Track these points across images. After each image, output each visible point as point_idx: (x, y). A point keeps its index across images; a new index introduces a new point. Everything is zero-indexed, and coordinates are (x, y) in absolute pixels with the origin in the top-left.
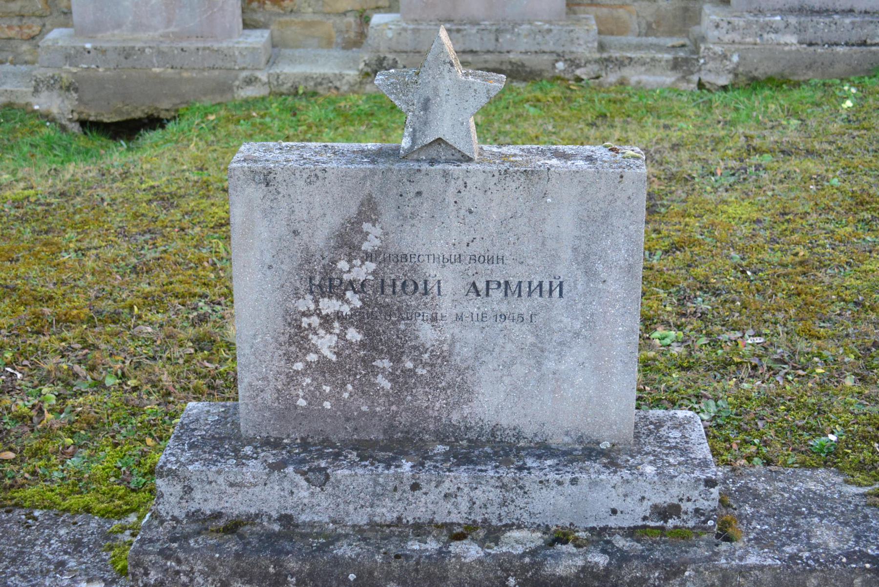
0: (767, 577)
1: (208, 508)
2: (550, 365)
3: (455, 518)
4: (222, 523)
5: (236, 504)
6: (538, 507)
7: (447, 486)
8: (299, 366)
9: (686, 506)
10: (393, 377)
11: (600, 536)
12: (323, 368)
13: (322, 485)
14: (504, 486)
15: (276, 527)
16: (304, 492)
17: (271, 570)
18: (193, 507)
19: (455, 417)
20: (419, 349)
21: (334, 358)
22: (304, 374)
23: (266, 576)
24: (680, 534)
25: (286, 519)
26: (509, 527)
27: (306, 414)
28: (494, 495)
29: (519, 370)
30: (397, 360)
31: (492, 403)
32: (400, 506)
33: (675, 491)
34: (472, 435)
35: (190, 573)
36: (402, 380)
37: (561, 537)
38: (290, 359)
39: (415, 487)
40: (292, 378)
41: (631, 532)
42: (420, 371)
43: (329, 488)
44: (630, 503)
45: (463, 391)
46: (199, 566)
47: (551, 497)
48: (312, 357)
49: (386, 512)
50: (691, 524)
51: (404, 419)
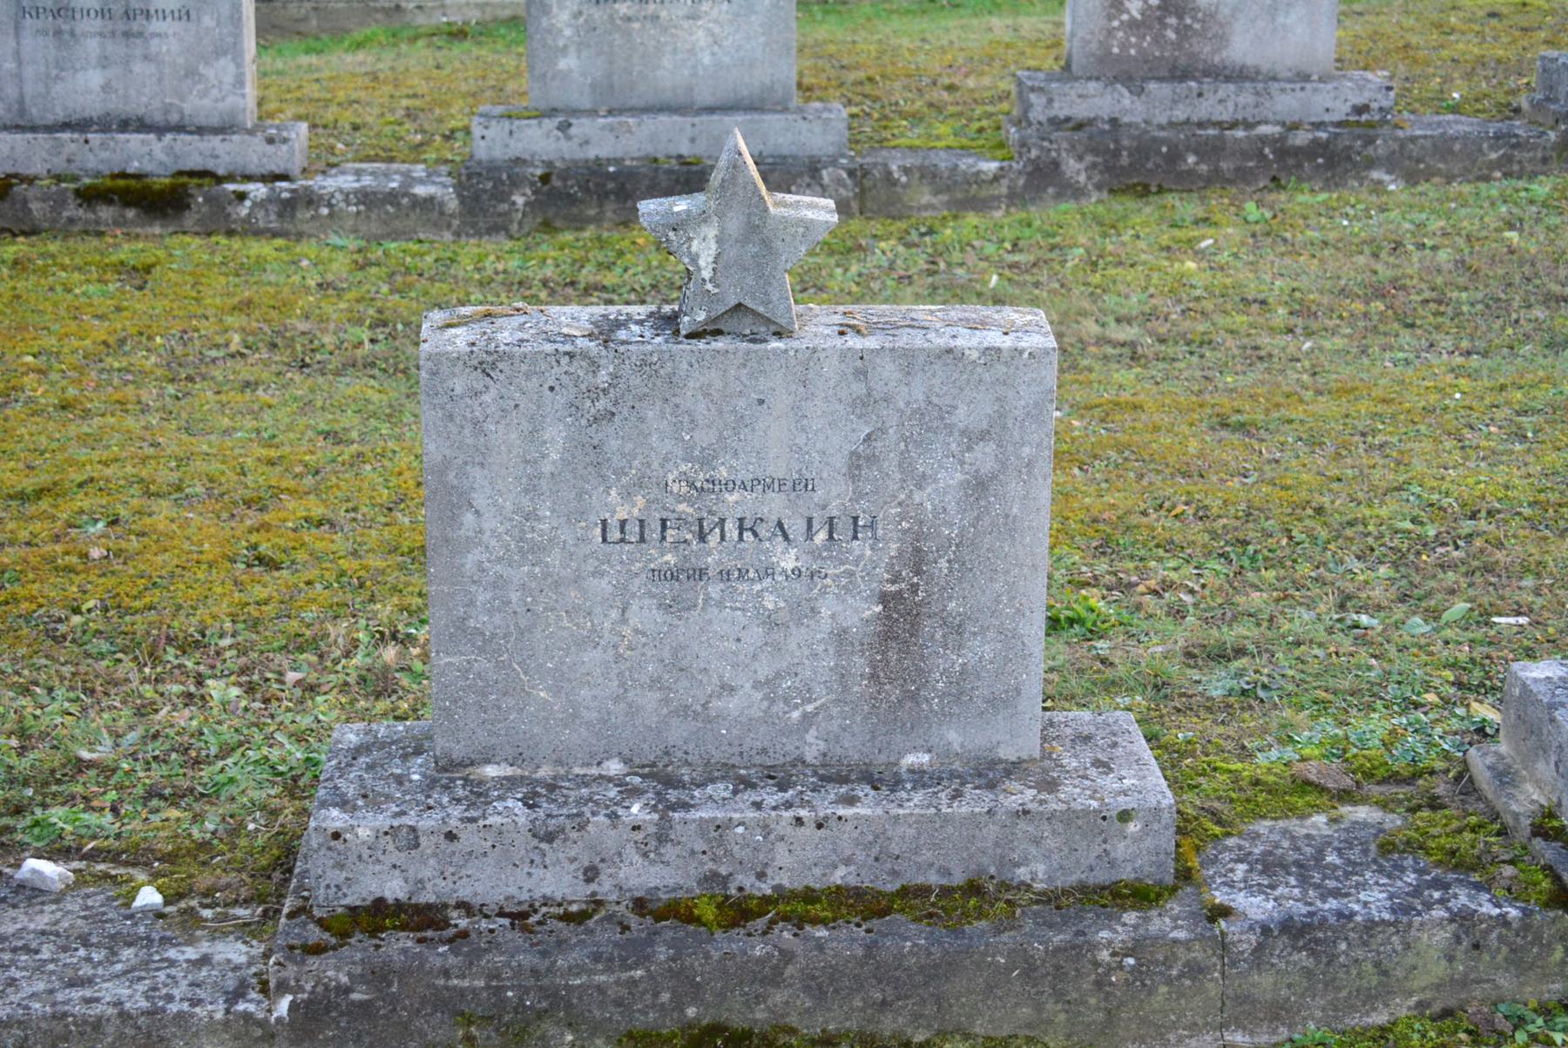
0: (1428, 144)
1: (1062, 115)
2: (1280, 19)
3: (1226, 117)
4: (1070, 125)
5: (1081, 111)
6: (1279, 107)
7: (1221, 94)
8: (1116, 23)
9: (1374, 105)
10: (1177, 31)
11: (1318, 126)
12: (1133, 25)
13: (1139, 95)
15: (1107, 127)
16: (1127, 100)
17: (1112, 146)
18: (1052, 113)
19: (1217, 59)
20: (1196, 9)
21: (1139, 17)
22: (1118, 29)
23: (1108, 150)
25: (1114, 121)
26: (1259, 123)
27: (1118, 58)
29: (1260, 24)
30: (1180, 18)
31: (1241, 48)
32: (1189, 110)
33: (1367, 94)
34: (1227, 72)
35: (1058, 151)
36: (1184, 32)
37: (1295, 126)
38: (1110, 18)
39: (1200, 95)
40: (1110, 32)
41: (1339, 124)
42: (1197, 26)
43: (1143, 97)
45: (1222, 40)
46: (1065, 145)
47: (1286, 103)
48: (1125, 17)
49: (1180, 114)
50: (1377, 118)
51: (1183, 61)
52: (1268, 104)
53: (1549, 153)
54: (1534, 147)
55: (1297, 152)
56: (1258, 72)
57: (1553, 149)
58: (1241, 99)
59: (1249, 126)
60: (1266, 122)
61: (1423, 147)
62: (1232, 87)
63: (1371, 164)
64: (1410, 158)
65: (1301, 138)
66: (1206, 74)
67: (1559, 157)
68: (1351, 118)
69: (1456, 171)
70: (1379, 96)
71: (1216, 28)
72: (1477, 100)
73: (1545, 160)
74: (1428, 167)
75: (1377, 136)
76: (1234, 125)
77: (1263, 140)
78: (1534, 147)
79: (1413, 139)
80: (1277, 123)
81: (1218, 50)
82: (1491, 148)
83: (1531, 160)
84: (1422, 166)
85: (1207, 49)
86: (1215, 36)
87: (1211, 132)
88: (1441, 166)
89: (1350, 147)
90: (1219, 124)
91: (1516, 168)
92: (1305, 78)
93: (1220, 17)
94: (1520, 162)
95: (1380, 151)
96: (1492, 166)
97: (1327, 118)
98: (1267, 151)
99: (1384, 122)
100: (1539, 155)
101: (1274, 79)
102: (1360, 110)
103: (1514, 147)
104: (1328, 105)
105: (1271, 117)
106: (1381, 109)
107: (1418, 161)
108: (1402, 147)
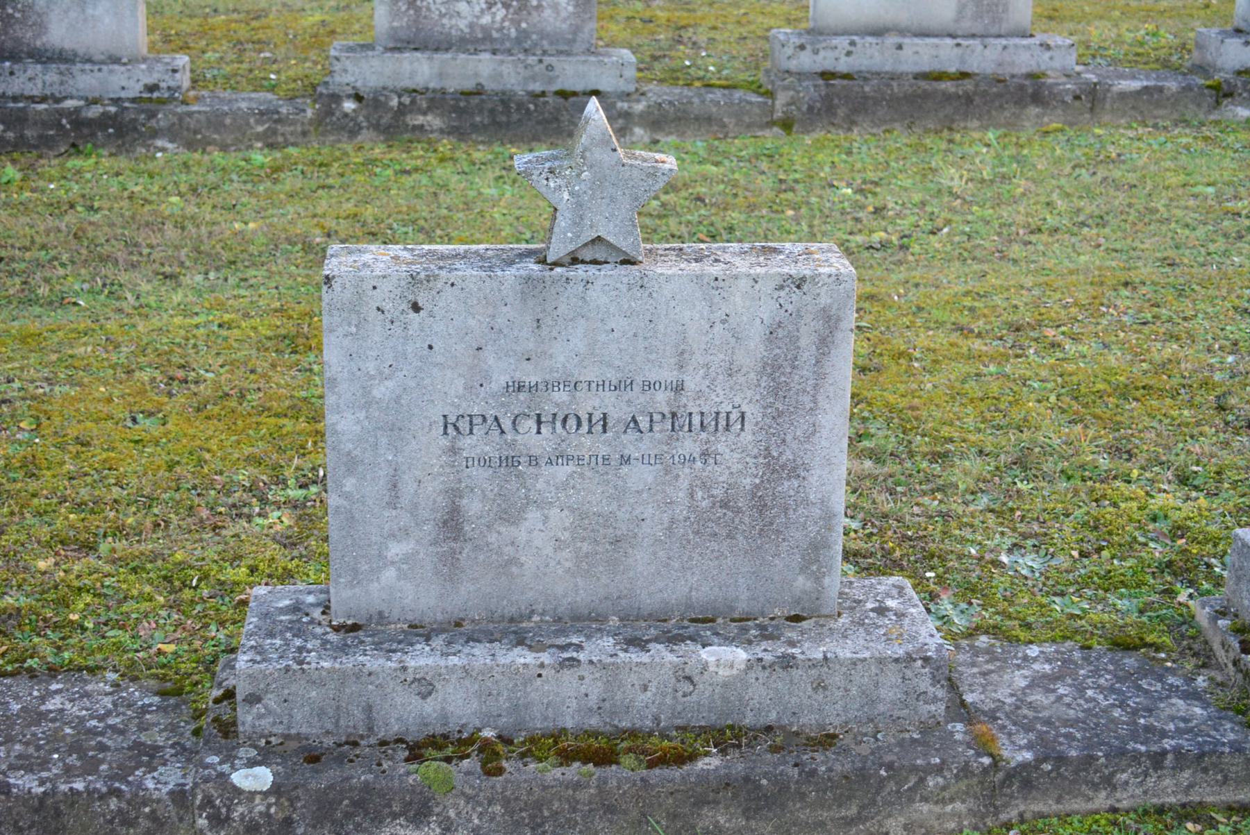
0: (202, 118)
2: (90, 11)
3: (35, 93)
6: (81, 86)
7: (30, 73)
9: (163, 85)
11: (116, 101)
14: (61, 73)
19: (38, 43)
24: (161, 102)
26: (65, 98)
28: (56, 78)
29: (73, 14)
31: (58, 34)
34: (49, 54)
37: (95, 101)
39: (12, 73)
41: (133, 100)
42: (18, 15)
44: (132, 83)
45: (41, 27)
47: (86, 81)
50: (166, 95)
52: (71, 82)
53: (307, 128)
54: (293, 123)
55: (90, 123)
56: (75, 55)
57: (310, 124)
58: (47, 77)
59: (58, 100)
60: (72, 98)
61: (198, 121)
62: (39, 67)
63: (155, 134)
64: (188, 129)
65: (94, 112)
66: (31, 55)
67: (316, 130)
68: (145, 95)
69: (229, 142)
70: (166, 77)
71: (34, 18)
72: (295, 81)
73: (304, 134)
74: (204, 137)
75: (158, 111)
76: (43, 99)
77: (62, 113)
78: (293, 123)
79: (190, 114)
80: (80, 98)
81: (36, 37)
82: (258, 122)
83: (292, 134)
84: (199, 137)
85: (29, 35)
86: (34, 24)
87: (21, 105)
88: (216, 136)
89: (135, 120)
90: (32, 99)
91: (280, 139)
92: (116, 60)
93: (37, 8)
94: (283, 135)
95: (161, 123)
96: (258, 137)
97: (123, 95)
98: (64, 121)
99: (172, 99)
100: (299, 129)
101: (89, 61)
102: (152, 88)
103: (276, 121)
104: (124, 84)
105: (74, 92)
106: (169, 88)
107: (196, 132)
108: (181, 119)
